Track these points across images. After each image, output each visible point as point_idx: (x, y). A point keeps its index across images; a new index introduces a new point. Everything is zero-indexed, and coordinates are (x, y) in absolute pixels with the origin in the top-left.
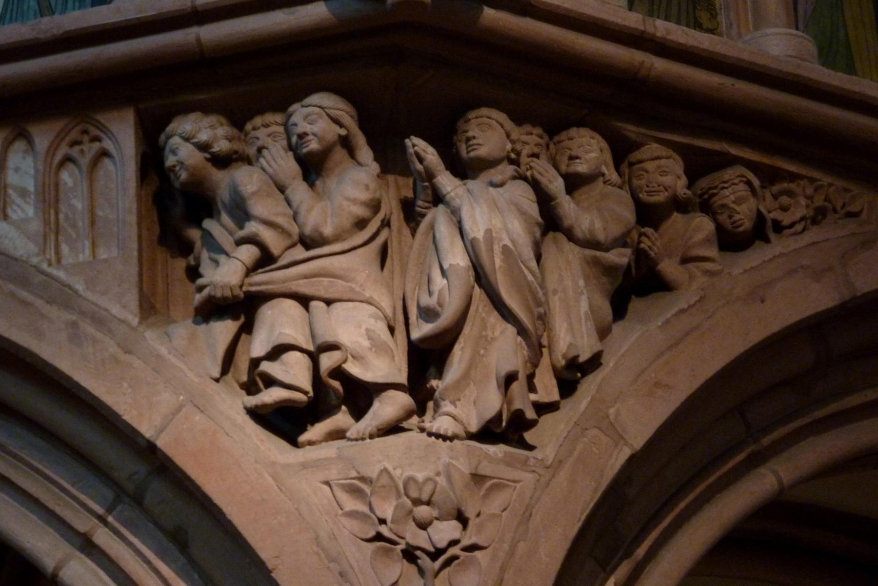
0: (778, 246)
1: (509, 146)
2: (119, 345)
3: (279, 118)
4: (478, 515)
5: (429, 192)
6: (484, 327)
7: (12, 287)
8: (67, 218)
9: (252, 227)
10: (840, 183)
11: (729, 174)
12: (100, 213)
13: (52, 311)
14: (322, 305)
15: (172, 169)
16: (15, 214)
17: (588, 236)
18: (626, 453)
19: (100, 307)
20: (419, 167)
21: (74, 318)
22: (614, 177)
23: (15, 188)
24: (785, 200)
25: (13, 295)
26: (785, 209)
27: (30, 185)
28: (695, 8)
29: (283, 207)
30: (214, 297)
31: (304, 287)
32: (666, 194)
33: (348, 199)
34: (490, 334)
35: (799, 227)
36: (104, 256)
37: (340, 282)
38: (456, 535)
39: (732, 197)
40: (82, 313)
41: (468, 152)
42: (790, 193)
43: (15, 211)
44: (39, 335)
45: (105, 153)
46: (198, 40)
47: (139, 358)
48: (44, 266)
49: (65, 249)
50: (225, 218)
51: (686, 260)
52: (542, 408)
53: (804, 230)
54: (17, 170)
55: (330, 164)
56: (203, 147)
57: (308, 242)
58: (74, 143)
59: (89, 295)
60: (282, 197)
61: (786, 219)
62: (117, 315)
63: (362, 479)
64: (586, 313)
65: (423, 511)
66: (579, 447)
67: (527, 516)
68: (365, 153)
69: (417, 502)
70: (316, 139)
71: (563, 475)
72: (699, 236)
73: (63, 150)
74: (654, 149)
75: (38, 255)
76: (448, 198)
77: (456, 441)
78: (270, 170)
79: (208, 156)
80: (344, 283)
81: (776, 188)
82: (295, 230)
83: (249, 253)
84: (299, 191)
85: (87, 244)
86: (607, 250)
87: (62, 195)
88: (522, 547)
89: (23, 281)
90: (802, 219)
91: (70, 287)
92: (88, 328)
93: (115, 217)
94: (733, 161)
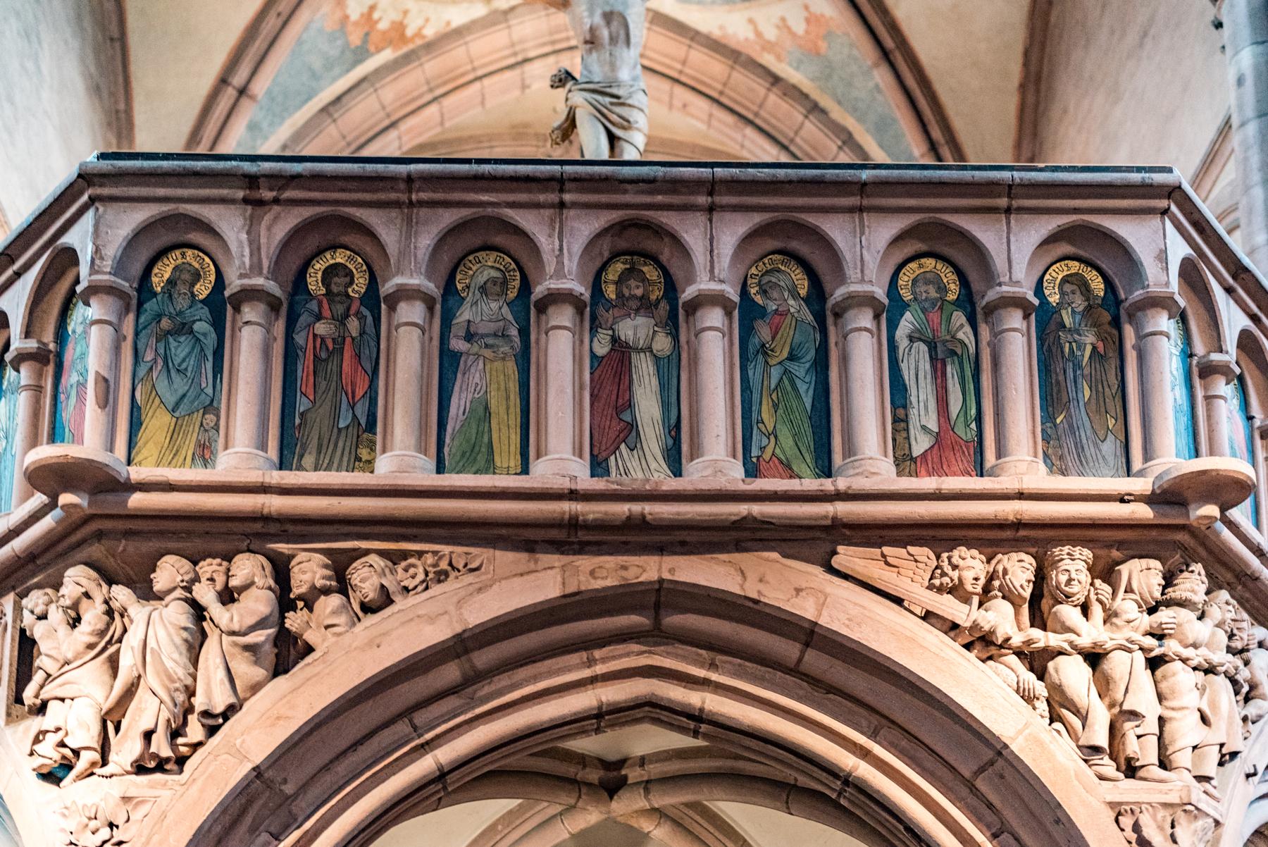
0: (401, 603)
1: (180, 578)
4: (128, 820)
6: (140, 702)
18: (250, 766)
24: (412, 571)
26: (413, 577)
28: (357, 447)
34: (143, 706)
35: (420, 588)
38: (107, 837)
51: (327, 627)
52: (196, 746)
53: (427, 588)
61: (410, 583)
63: (66, 808)
64: (222, 680)
65: (93, 824)
66: (211, 769)
67: (164, 816)
69: (90, 819)
71: (194, 790)
72: (329, 610)
74: (302, 556)
77: (114, 778)
81: (404, 564)
86: (245, 634)
88: (156, 838)
90: (423, 582)
94: (367, 552)
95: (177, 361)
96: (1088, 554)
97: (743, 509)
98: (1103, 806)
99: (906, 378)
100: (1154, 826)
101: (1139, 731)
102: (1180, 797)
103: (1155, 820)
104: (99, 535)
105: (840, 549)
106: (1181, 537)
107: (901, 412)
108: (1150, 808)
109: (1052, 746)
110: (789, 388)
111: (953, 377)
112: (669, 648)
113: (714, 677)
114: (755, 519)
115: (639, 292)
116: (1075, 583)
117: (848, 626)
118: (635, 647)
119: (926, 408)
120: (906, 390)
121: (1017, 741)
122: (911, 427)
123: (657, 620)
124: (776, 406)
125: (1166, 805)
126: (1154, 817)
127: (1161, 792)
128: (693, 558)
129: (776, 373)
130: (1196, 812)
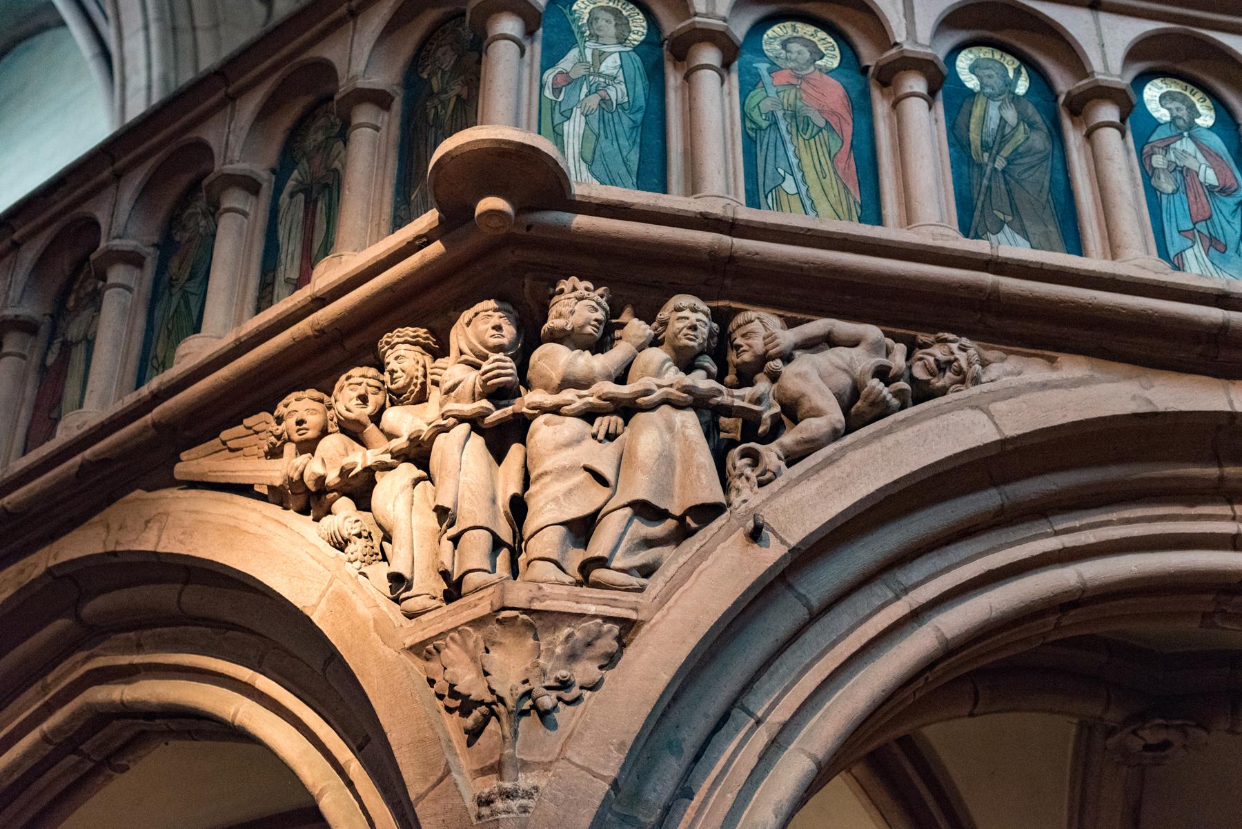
96: (409, 331)
97: (78, 459)
98: (403, 656)
99: (281, 239)
100: (466, 659)
101: (452, 532)
102: (492, 604)
103: (467, 651)
105: (184, 456)
106: (510, 257)
107: (269, 279)
108: (456, 635)
109: (354, 597)
110: (183, 310)
111: (321, 212)
112: (106, 644)
113: (137, 659)
114: (89, 462)
115: (90, 289)
116: (400, 373)
117: (181, 542)
118: (80, 655)
119: (292, 259)
120: (278, 250)
121: (319, 608)
122: (276, 287)
123: (77, 616)
124: (170, 332)
125: (477, 623)
126: (464, 646)
127: (469, 606)
128: (75, 532)
129: (175, 301)
130: (525, 617)
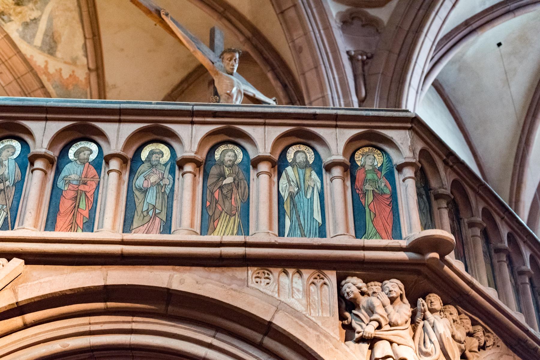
2: (334, 346)
3: (380, 284)
5: (423, 316)
7: (296, 320)
8: (312, 300)
9: (375, 316)
10: (497, 336)
11: (480, 327)
12: (323, 302)
13: (311, 330)
14: (397, 345)
15: (348, 293)
16: (296, 297)
17: (459, 339)
19: (327, 332)
20: (423, 308)
21: (318, 334)
22: (459, 321)
23: (296, 289)
25: (297, 322)
27: (301, 289)
29: (385, 312)
30: (365, 336)
31: (392, 338)
32: (468, 330)
33: (405, 314)
35: (491, 347)
36: (325, 316)
37: (402, 339)
39: (480, 335)
40: (321, 333)
41: (431, 306)
42: (488, 337)
43: (295, 296)
44: (306, 337)
45: (325, 284)
46: (364, 255)
47: (340, 351)
48: (307, 315)
49: (312, 311)
50: (363, 311)
51: (470, 351)
54: (296, 283)
55: (396, 301)
56: (359, 288)
57: (391, 324)
58: (316, 278)
59: (322, 327)
60: (384, 309)
62: (333, 336)
68: (405, 300)
70: (395, 293)
73: (312, 280)
75: (305, 311)
76: (429, 319)
78: (382, 300)
79: (360, 291)
80: (404, 340)
82: (388, 320)
83: (376, 324)
84: (390, 307)
85: (320, 311)
87: (311, 294)
89: (301, 319)
91: (316, 324)
92: (323, 338)
93: (329, 304)
95: (422, 208)
104: (419, 273)
